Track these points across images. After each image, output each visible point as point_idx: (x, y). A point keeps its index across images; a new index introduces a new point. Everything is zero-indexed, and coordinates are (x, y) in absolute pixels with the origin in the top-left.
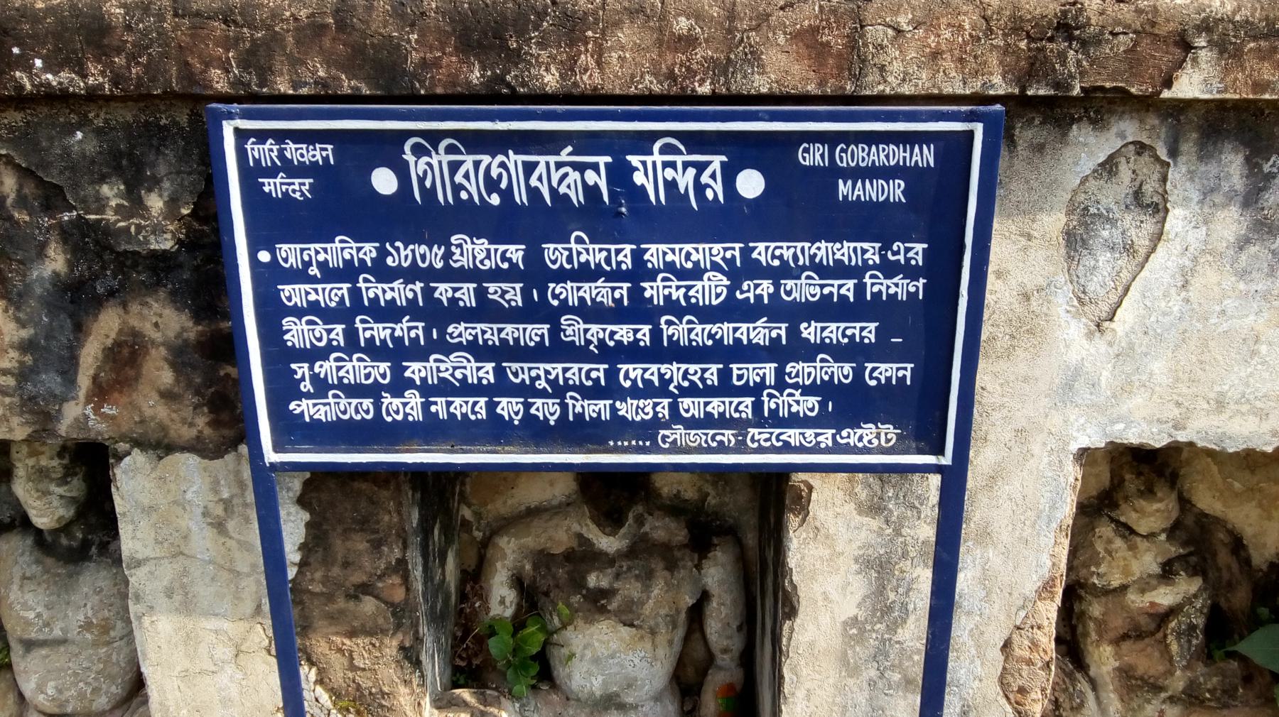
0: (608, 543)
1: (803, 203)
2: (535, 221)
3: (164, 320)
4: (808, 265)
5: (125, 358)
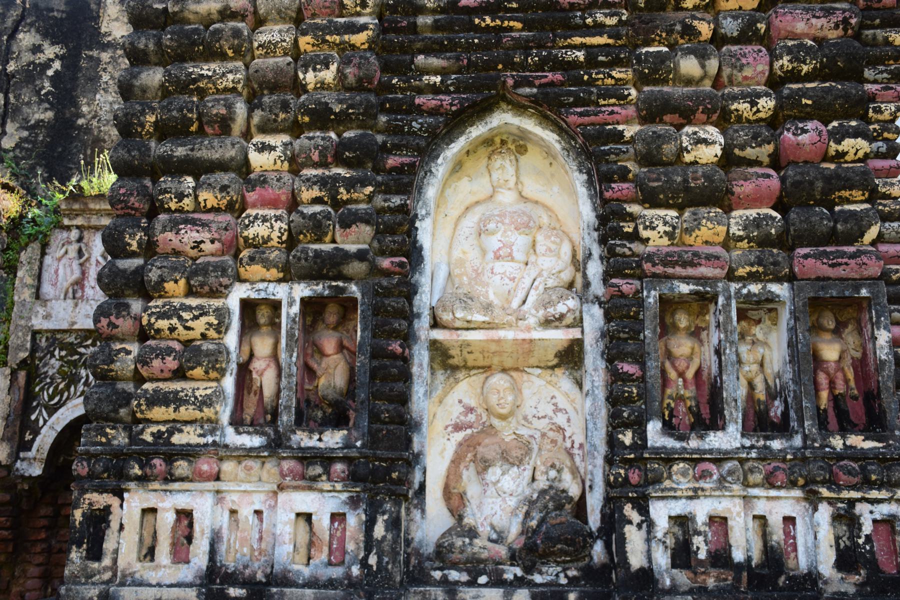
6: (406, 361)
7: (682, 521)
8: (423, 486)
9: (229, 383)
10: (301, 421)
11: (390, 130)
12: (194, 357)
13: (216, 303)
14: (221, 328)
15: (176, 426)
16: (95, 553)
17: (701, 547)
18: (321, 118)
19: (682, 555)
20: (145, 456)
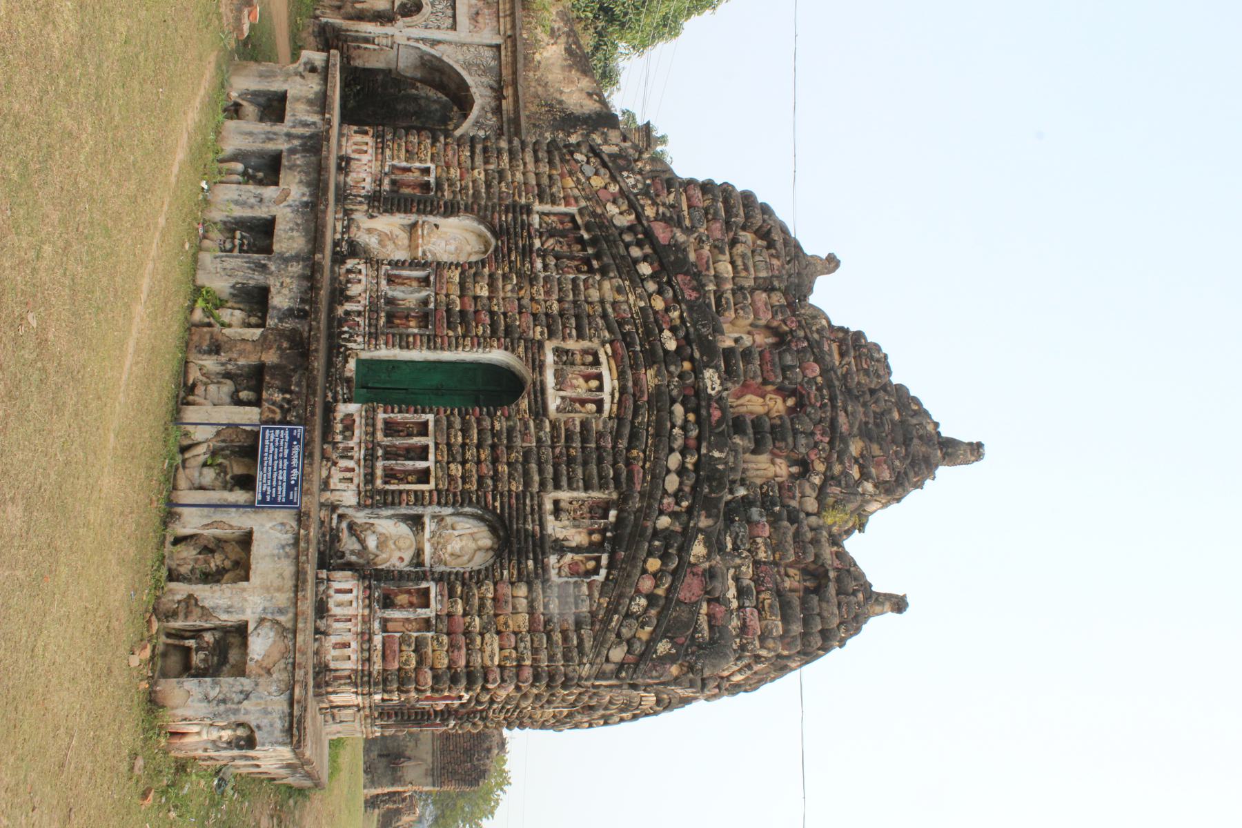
0: (228, 477)
1: (290, 488)
2: (290, 458)
3: (278, 417)
4: (283, 489)
5: (273, 412)
6: (411, 212)
7: (360, 272)
8: (372, 217)
9: (404, 164)
10: (393, 182)
11: (486, 206)
12: (410, 155)
13: (429, 159)
14: (421, 161)
15: (392, 150)
16: (356, 132)
17: (351, 276)
18: (488, 186)
19: (349, 271)
20: (383, 142)
